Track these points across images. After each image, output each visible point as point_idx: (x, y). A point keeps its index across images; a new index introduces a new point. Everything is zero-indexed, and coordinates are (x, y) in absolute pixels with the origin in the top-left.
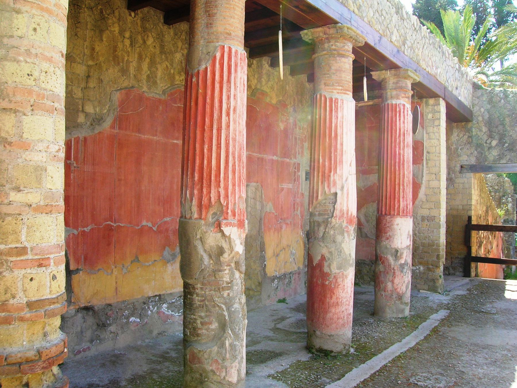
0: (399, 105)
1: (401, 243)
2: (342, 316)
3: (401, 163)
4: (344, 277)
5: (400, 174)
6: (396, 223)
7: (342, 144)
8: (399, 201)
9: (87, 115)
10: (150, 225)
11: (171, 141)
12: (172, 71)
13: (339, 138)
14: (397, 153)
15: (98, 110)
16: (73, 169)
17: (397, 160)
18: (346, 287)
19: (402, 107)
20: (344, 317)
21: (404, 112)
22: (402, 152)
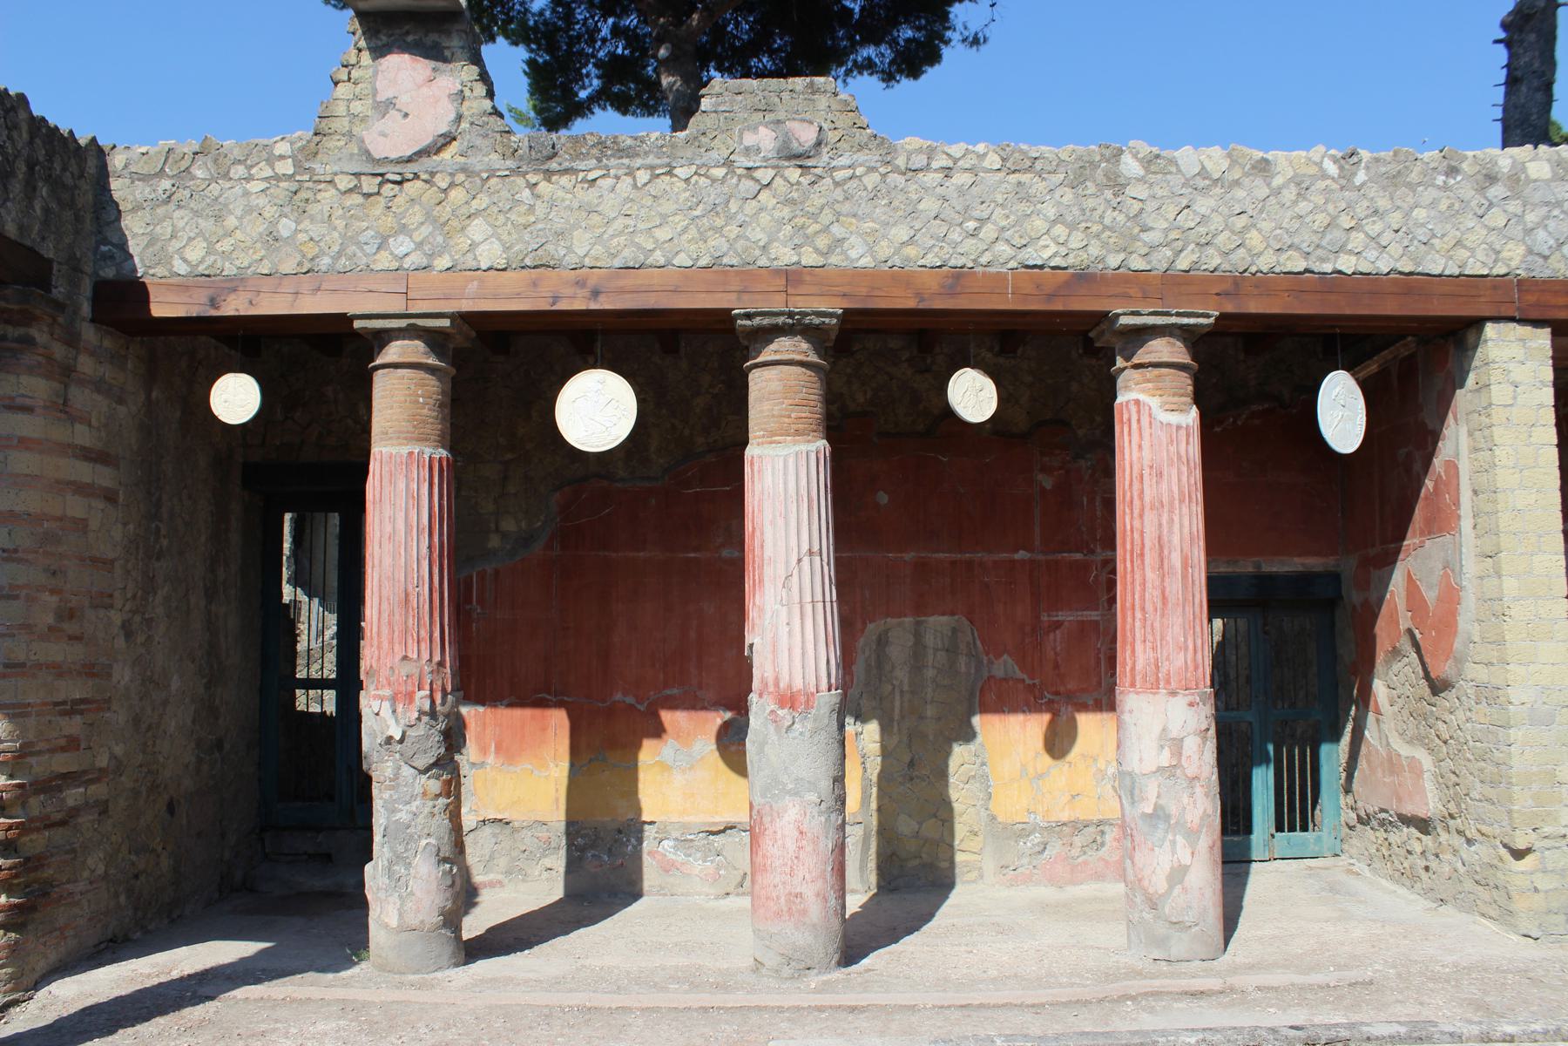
0: (1127, 402)
1: (1141, 760)
2: (774, 895)
3: (1137, 550)
4: (775, 814)
5: (1133, 582)
6: (1127, 708)
7: (762, 546)
8: (1133, 651)
9: (504, 536)
10: (630, 700)
11: (681, 555)
12: (687, 432)
13: (758, 533)
14: (1128, 527)
15: (523, 524)
16: (475, 616)
17: (1128, 547)
18: (779, 835)
19: (1133, 409)
20: (778, 897)
21: (1139, 421)
22: (1137, 524)
